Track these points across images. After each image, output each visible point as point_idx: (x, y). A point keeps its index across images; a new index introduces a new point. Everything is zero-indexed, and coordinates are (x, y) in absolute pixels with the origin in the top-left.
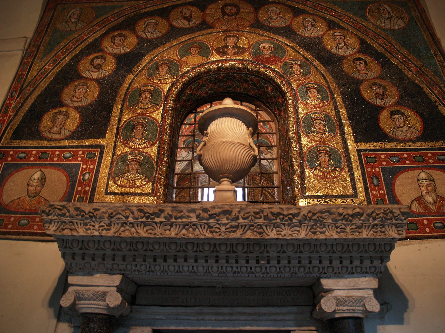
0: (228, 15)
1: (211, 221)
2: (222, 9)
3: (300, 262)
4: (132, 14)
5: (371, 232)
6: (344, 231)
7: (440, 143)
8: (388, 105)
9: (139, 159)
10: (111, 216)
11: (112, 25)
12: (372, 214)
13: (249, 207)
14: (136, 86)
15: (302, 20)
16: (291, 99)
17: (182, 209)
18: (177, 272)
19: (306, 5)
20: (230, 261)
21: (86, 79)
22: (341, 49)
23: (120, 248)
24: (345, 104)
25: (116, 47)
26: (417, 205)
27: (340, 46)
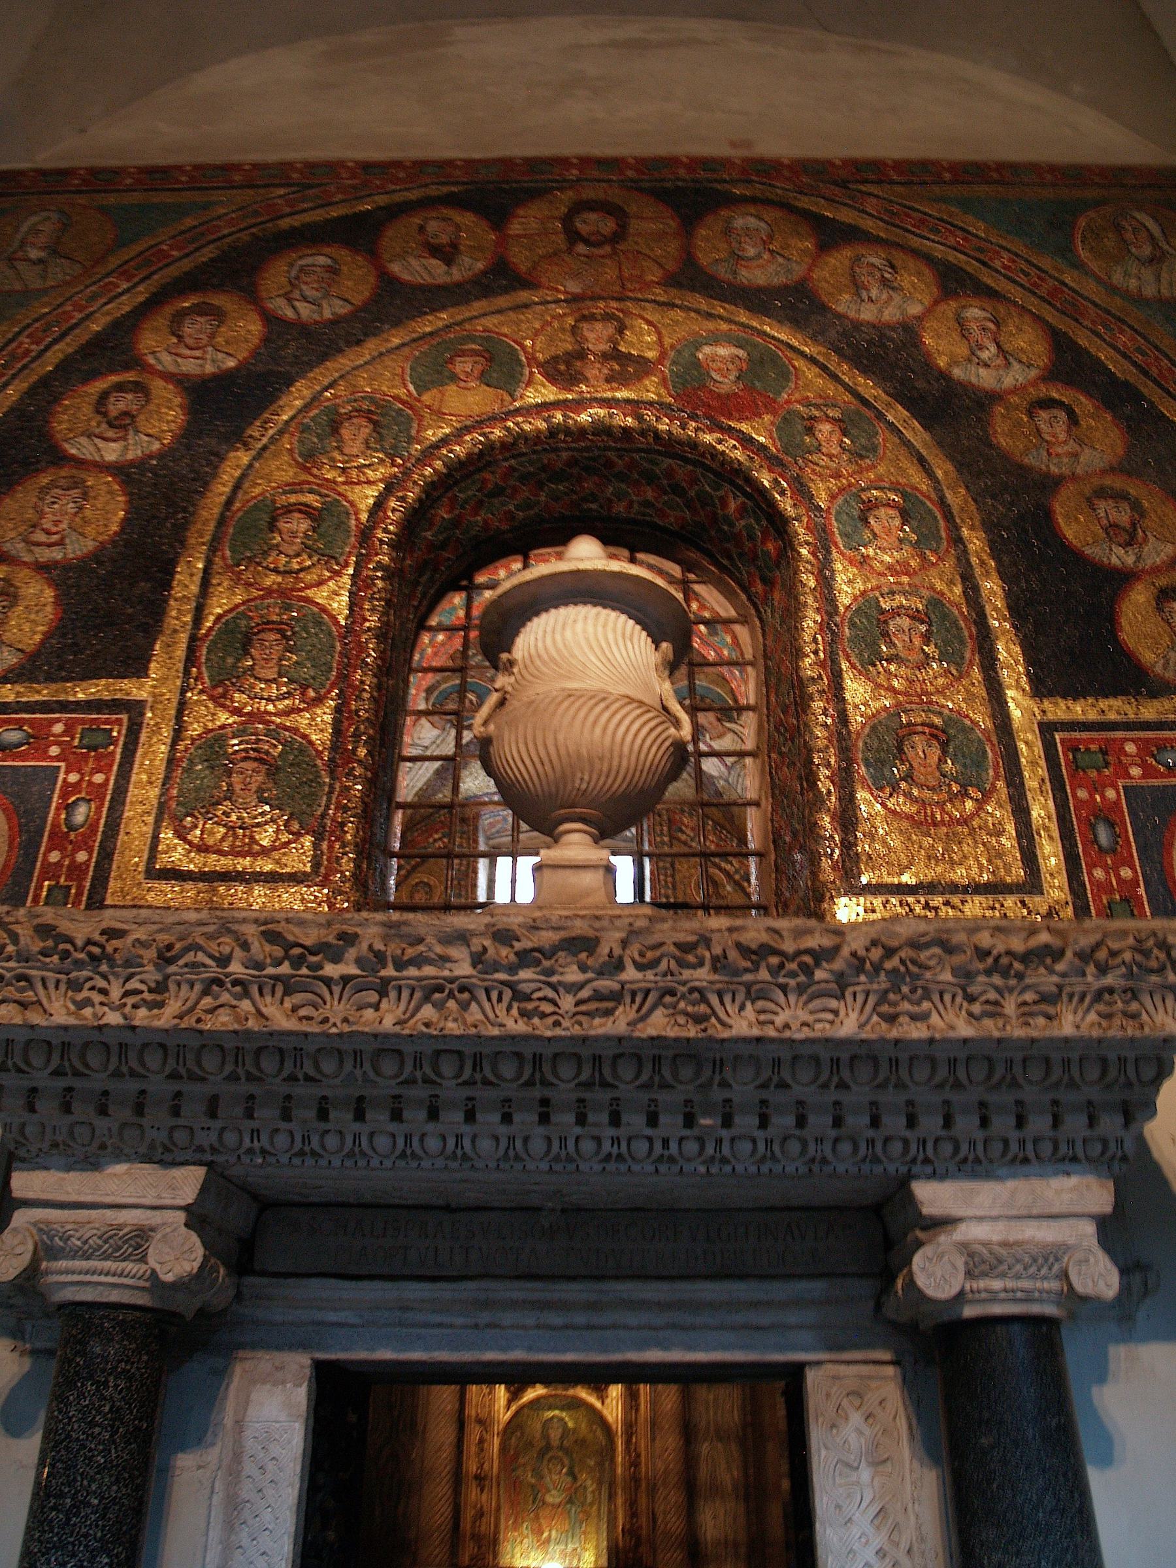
0: (587, 242)
1: (525, 974)
2: (567, 220)
3: (838, 1122)
4: (245, 236)
5: (1092, 1016)
6: (994, 1010)
9: (267, 753)
10: (169, 955)
11: (173, 271)
12: (1093, 951)
13: (659, 926)
14: (258, 490)
15: (847, 262)
16: (808, 543)
17: (422, 931)
18: (403, 1155)
20: (591, 1118)
21: (81, 463)
22: (986, 365)
23: (196, 1070)
24: (999, 561)
25: (188, 352)
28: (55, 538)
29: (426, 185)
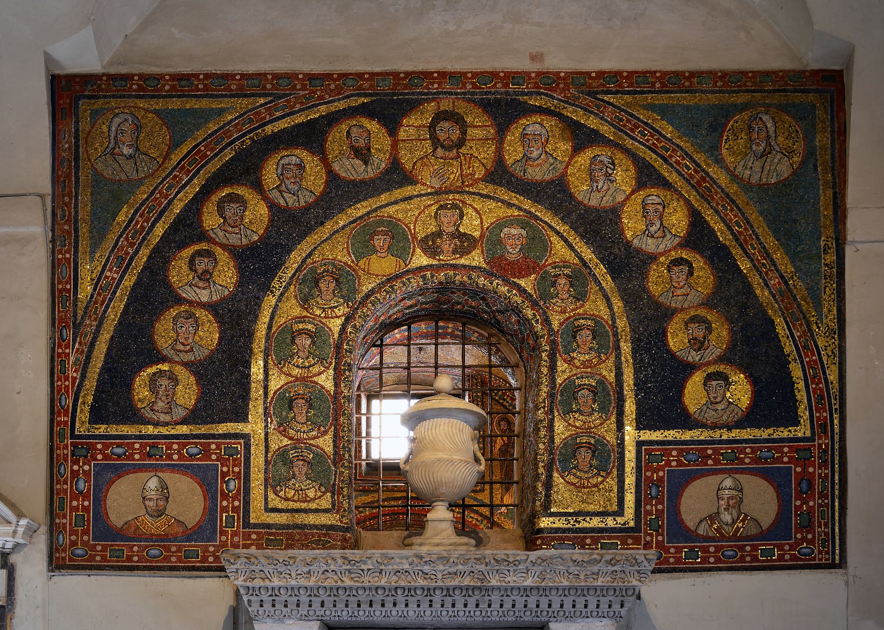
0: (443, 147)
2: (432, 127)
8: (707, 361)
11: (213, 167)
14: (283, 320)
15: (588, 162)
16: (546, 351)
19: (603, 118)
21: (191, 303)
22: (652, 236)
27: (651, 229)
28: (188, 347)
29: (348, 97)
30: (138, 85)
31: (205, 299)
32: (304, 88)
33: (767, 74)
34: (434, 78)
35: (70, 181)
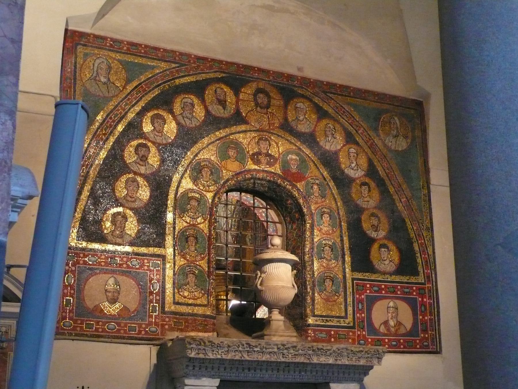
7: (408, 278)
16: (309, 223)
21: (135, 173)
22: (353, 169)
26: (384, 327)
30: (110, 43)
31: (143, 172)
32: (194, 63)
33: (394, 97)
34: (256, 70)
35: (71, 91)
